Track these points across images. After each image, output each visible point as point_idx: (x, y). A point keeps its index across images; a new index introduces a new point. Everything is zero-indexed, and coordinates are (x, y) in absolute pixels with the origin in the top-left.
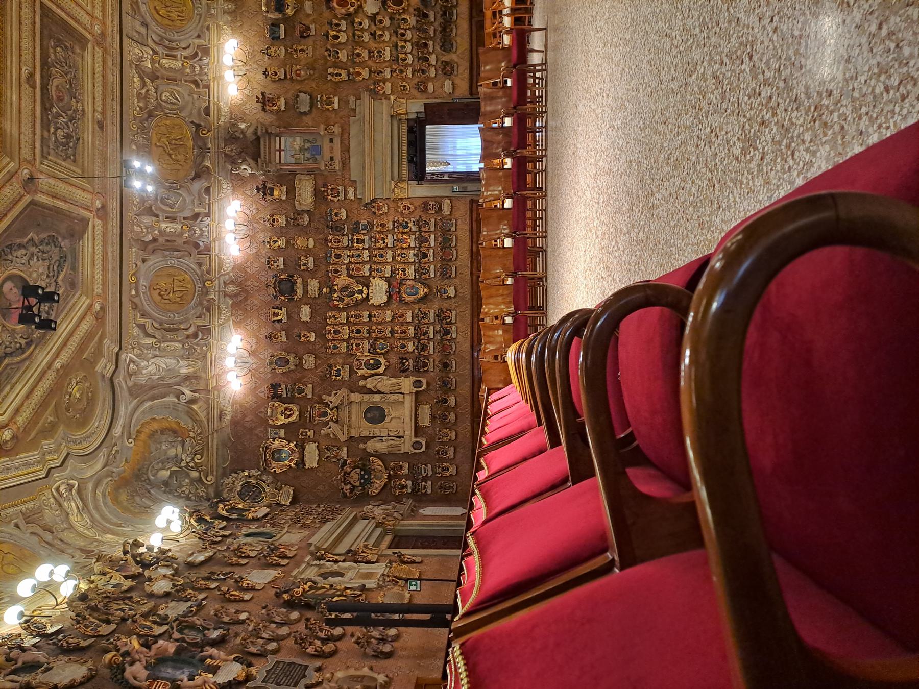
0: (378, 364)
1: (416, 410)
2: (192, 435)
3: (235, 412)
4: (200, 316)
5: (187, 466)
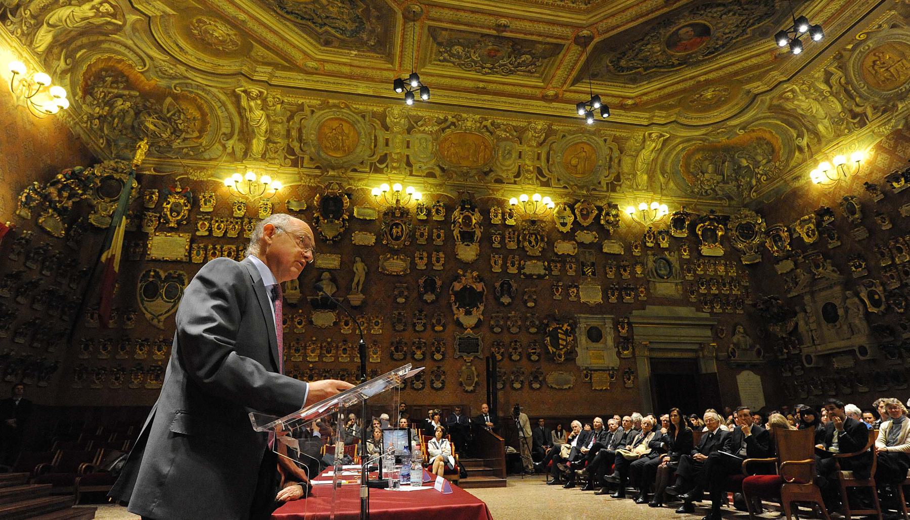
0: (876, 304)
1: (844, 352)
2: (777, 164)
3: (801, 188)
4: (875, 108)
5: (757, 174)
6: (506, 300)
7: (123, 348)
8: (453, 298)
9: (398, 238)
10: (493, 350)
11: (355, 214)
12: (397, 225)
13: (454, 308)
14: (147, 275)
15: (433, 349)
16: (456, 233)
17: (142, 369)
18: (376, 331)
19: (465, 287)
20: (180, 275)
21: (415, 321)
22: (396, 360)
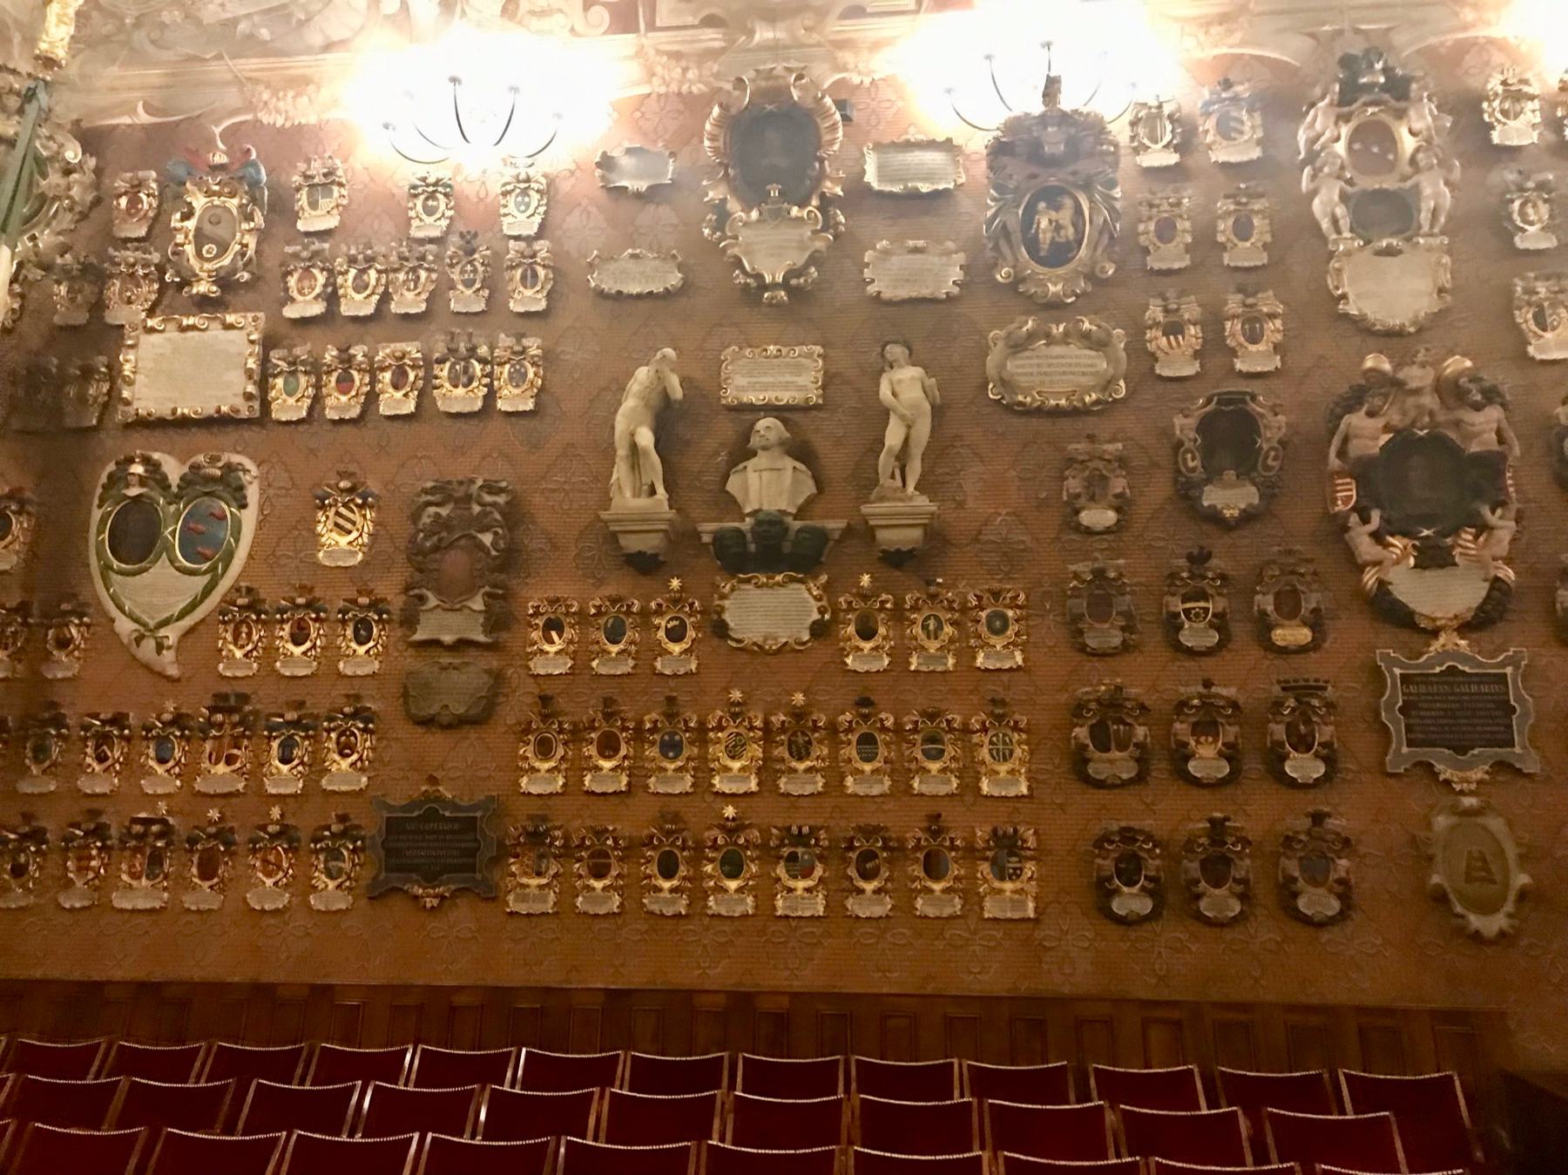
7: (40, 752)
8: (1347, 493)
9: (1059, 254)
11: (871, 177)
12: (1052, 197)
14: (119, 479)
15: (1279, 731)
16: (1326, 204)
17: (100, 832)
18: (998, 654)
19: (1403, 443)
20: (229, 468)
22: (1100, 785)
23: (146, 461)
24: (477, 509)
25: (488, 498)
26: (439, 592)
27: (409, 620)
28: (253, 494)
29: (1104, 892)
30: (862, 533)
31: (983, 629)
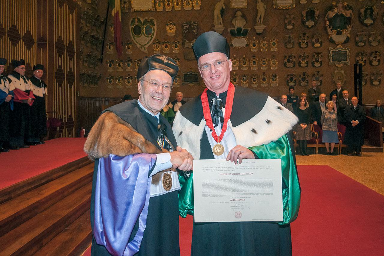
6: (369, 21)
8: (328, 23)
10: (358, 58)
13: (329, 30)
18: (274, 49)
19: (337, 15)
21: (301, 41)
23: (138, 18)
24: (192, 26)
25: (194, 25)
26: (188, 40)
27: (184, 44)
28: (155, 24)
29: (288, 82)
30: (255, 30)
31: (272, 45)
